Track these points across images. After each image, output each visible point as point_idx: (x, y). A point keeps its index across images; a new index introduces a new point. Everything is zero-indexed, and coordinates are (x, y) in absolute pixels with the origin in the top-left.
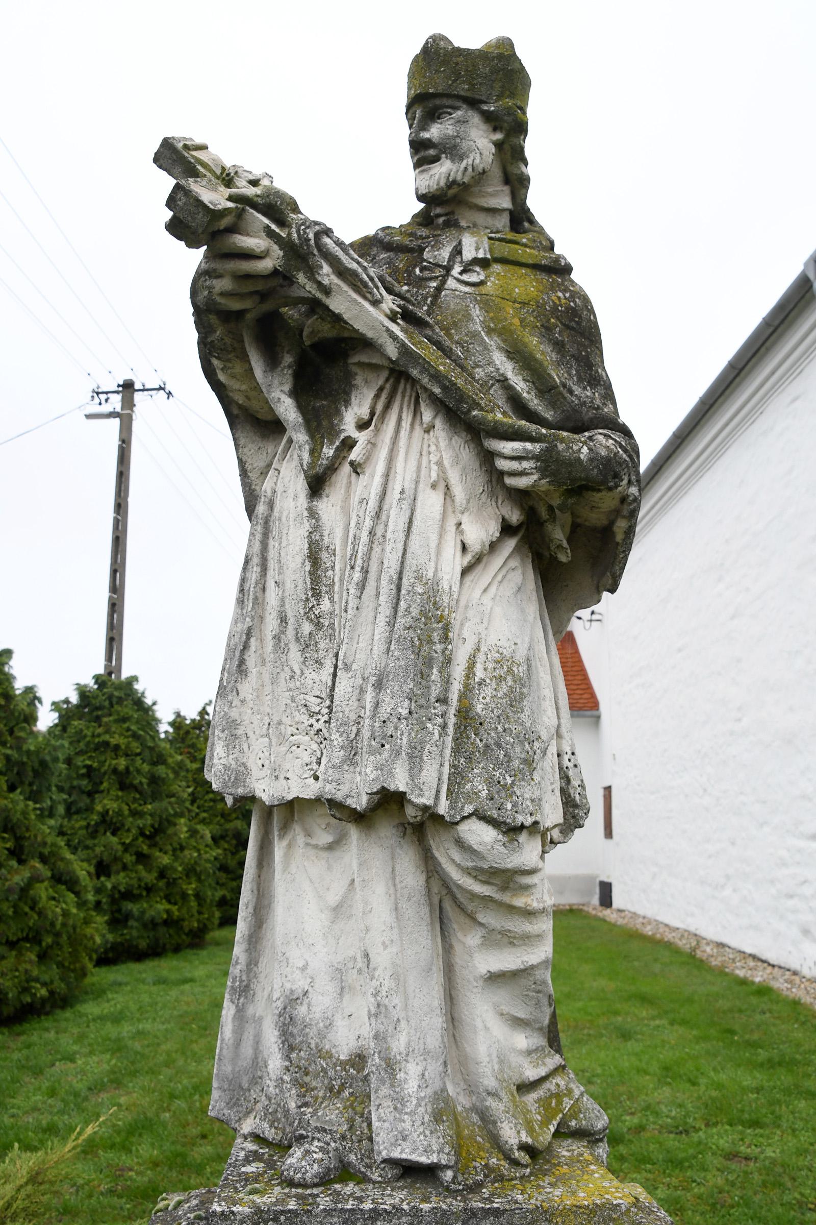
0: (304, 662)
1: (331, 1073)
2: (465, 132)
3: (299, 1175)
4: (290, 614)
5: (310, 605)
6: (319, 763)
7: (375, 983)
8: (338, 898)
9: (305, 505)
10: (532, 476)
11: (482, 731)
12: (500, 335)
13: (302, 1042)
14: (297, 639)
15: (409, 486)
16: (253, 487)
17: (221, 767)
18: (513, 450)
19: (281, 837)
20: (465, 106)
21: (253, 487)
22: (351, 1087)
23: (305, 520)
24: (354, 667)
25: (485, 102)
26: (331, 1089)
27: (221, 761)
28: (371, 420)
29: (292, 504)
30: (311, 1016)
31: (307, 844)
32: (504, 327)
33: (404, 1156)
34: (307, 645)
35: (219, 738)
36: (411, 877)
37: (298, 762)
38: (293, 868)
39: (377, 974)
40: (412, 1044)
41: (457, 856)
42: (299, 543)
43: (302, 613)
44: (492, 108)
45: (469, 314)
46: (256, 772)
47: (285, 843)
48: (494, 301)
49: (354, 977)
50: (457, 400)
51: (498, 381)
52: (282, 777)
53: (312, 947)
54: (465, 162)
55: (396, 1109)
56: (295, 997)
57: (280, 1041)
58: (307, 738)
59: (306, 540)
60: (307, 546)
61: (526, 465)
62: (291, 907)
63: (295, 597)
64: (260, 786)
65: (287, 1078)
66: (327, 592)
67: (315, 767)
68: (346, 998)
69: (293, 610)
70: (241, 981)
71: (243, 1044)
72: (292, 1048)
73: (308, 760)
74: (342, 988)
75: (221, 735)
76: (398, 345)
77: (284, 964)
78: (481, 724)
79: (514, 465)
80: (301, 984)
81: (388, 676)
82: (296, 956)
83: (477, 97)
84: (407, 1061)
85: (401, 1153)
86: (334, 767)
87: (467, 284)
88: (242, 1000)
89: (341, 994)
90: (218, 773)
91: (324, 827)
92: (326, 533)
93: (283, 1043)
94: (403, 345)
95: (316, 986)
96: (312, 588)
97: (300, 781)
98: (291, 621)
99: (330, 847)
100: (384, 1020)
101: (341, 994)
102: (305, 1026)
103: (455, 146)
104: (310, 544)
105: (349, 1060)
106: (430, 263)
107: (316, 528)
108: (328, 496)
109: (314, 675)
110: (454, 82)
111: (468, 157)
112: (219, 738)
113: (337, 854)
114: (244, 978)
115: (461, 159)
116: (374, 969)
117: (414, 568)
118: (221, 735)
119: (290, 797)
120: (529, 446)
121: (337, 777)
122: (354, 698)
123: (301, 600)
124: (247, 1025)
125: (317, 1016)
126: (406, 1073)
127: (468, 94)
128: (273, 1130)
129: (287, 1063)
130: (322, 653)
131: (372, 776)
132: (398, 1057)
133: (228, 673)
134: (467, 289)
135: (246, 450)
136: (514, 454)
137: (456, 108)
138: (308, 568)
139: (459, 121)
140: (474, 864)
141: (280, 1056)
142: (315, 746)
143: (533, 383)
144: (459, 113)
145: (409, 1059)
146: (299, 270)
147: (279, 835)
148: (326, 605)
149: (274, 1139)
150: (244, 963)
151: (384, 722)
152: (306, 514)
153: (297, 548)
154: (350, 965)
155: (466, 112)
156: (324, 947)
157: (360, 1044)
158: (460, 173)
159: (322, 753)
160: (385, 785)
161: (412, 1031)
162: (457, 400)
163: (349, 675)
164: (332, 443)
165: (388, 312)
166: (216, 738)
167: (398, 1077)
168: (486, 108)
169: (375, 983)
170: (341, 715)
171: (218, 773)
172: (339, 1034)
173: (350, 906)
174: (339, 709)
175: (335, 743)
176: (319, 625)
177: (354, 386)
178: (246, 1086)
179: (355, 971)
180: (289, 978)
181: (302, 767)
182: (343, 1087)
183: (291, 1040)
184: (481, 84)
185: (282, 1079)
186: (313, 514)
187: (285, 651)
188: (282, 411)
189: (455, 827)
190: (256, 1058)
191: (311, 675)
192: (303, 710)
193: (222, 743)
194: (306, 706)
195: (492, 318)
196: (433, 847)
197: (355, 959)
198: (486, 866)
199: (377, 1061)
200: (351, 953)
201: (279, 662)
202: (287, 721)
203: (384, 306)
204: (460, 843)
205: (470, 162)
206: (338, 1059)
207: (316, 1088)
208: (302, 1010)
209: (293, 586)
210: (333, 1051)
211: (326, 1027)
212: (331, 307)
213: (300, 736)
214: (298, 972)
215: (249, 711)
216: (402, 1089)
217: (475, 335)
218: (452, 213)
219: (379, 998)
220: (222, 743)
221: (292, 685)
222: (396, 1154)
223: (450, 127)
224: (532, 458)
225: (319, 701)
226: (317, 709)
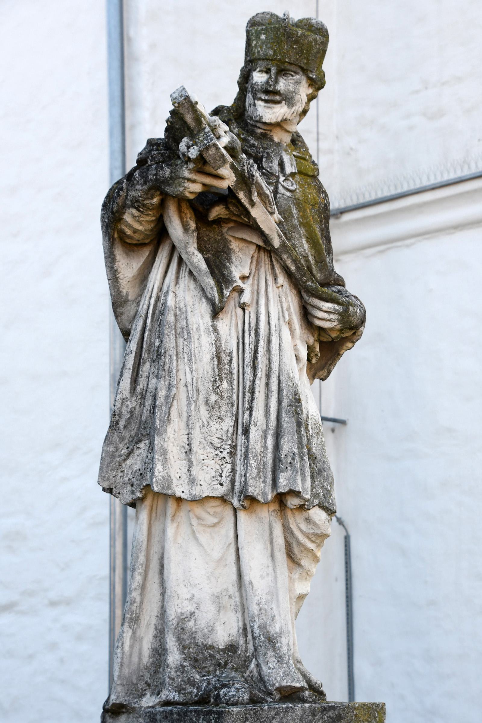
0: (210, 418)
1: (218, 656)
2: (298, 89)
3: (241, 698)
4: (201, 388)
5: (218, 385)
6: (221, 476)
7: (257, 598)
8: (220, 555)
9: (210, 324)
10: (333, 323)
11: (316, 462)
12: (305, 227)
13: (190, 643)
14: (207, 403)
15: (277, 322)
16: (121, 289)
17: (161, 477)
18: (328, 308)
19: (173, 521)
20: (301, 73)
21: (121, 289)
22: (231, 662)
23: (212, 333)
24: (258, 424)
25: (311, 72)
26: (219, 665)
27: (160, 474)
28: (248, 277)
29: (201, 321)
30: (196, 627)
31: (199, 524)
32: (307, 223)
33: (289, 684)
34: (212, 407)
35: (159, 460)
36: (280, 540)
37: (208, 477)
38: (180, 540)
39: (257, 593)
40: (283, 628)
41: (304, 527)
42: (208, 346)
43: (211, 389)
44: (314, 77)
45: (292, 212)
46: (175, 481)
47: (175, 525)
48: (302, 204)
49: (226, 600)
50: (302, 275)
51: (304, 257)
52: (199, 485)
53: (198, 586)
54: (294, 108)
55: (278, 661)
56: (183, 617)
57: (177, 644)
58: (213, 462)
59: (214, 346)
60: (214, 349)
61: (332, 316)
62: (180, 563)
63: (206, 379)
64: (179, 489)
65: (185, 664)
66: (225, 378)
67: (219, 478)
68: (222, 612)
69: (205, 386)
70: (136, 614)
71: (133, 655)
72: (184, 648)
73: (214, 475)
74: (220, 607)
75: (160, 458)
76: (281, 241)
77: (176, 597)
78: (315, 458)
79: (326, 316)
80: (188, 607)
81: (284, 431)
82: (184, 593)
83: (310, 69)
84: (281, 637)
85: (287, 683)
86: (253, 478)
87: (288, 190)
88: (135, 626)
89: (219, 611)
90: (159, 481)
91: (212, 513)
92: (223, 342)
93: (179, 645)
94: (283, 241)
95: (202, 608)
96: (219, 375)
97: (209, 486)
98: (203, 393)
99: (215, 525)
100: (264, 617)
101: (219, 611)
102: (192, 633)
103: (292, 98)
104: (216, 348)
105: (226, 648)
106: (268, 171)
107: (218, 339)
108: (222, 319)
109: (217, 425)
110: (300, 57)
111: (296, 105)
112: (159, 460)
113: (216, 529)
114: (138, 612)
115: (293, 106)
116: (256, 590)
117: (286, 372)
118: (160, 458)
119: (204, 496)
120: (336, 307)
121: (254, 484)
122: (260, 441)
123: (211, 381)
124: (136, 642)
125: (203, 626)
126: (281, 643)
127: (305, 67)
128: (182, 695)
129: (184, 656)
130: (223, 414)
131: (284, 484)
132: (275, 636)
133: (160, 421)
134: (288, 194)
135: (120, 264)
136: (328, 310)
137: (296, 73)
138: (216, 363)
139: (297, 82)
140: (313, 531)
141: (178, 652)
142: (218, 467)
143: (315, 257)
144: (298, 77)
145: (283, 636)
146: (241, 190)
147: (172, 520)
148: (225, 386)
149: (183, 700)
150: (139, 602)
151: (286, 455)
152: (211, 329)
153: (207, 350)
154: (224, 594)
155: (301, 77)
156: (208, 584)
157: (230, 639)
158: (290, 115)
159: (222, 471)
160: (292, 488)
161: (283, 621)
162: (302, 275)
163: (256, 428)
164: (229, 288)
165: (277, 220)
166: (157, 460)
167: (277, 645)
168: (311, 76)
169: (257, 598)
170: (254, 450)
171: (159, 481)
172: (218, 634)
173: (226, 560)
174: (253, 447)
175: (253, 465)
176: (222, 397)
177: (231, 249)
178: (135, 682)
179: (227, 597)
180: (180, 606)
181: (211, 479)
182: (226, 663)
183: (183, 643)
184: (312, 60)
185: (183, 666)
186: (215, 330)
187: (197, 409)
188: (195, 261)
189: (308, 511)
190: (139, 664)
191: (214, 425)
192: (210, 446)
193: (161, 464)
194: (211, 443)
195: (301, 216)
196: (291, 523)
197: (227, 590)
198: (319, 532)
199: (263, 639)
200: (225, 587)
201: (196, 417)
202: (201, 451)
203: (275, 216)
204: (308, 520)
205: (297, 109)
206: (219, 648)
207: (206, 667)
208: (191, 624)
209: (206, 372)
210: (215, 645)
211: (210, 632)
212: (252, 214)
213: (209, 461)
214: (186, 601)
215: (172, 444)
216: (280, 652)
217: (294, 227)
218: (271, 131)
219: (261, 606)
220: (161, 464)
221: (203, 431)
222: (284, 684)
223: (291, 85)
224: (337, 314)
225: (220, 441)
226: (219, 445)
